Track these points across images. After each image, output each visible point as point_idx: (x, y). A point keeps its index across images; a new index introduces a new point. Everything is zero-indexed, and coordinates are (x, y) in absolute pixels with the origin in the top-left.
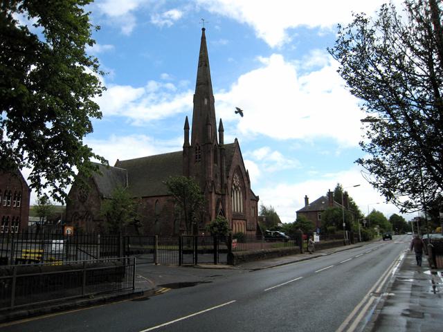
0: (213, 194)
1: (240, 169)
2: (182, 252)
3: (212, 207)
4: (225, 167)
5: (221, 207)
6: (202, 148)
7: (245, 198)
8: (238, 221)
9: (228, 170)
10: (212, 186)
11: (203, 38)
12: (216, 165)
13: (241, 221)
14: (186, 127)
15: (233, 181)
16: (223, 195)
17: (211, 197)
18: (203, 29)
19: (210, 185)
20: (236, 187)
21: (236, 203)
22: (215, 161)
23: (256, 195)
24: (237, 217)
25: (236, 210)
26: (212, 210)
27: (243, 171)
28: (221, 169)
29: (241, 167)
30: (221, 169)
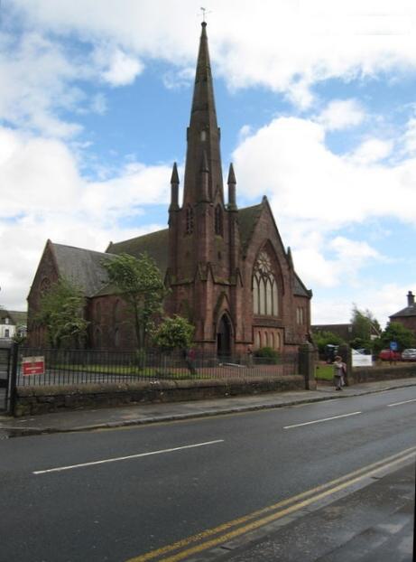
0: (209, 284)
1: (272, 246)
2: (78, 393)
3: (205, 305)
4: (237, 241)
5: (225, 305)
6: (194, 211)
7: (282, 292)
8: (266, 330)
9: (246, 247)
10: (207, 271)
11: (204, 38)
12: (219, 237)
13: (273, 330)
14: (175, 181)
15: (256, 264)
16: (232, 287)
17: (205, 290)
18: (204, 24)
19: (205, 268)
20: (263, 275)
21: (264, 299)
22: (218, 230)
23: (308, 289)
24: (262, 322)
25: (262, 312)
26: (206, 311)
27: (278, 249)
28: (231, 244)
29: (274, 242)
30: (231, 244)
